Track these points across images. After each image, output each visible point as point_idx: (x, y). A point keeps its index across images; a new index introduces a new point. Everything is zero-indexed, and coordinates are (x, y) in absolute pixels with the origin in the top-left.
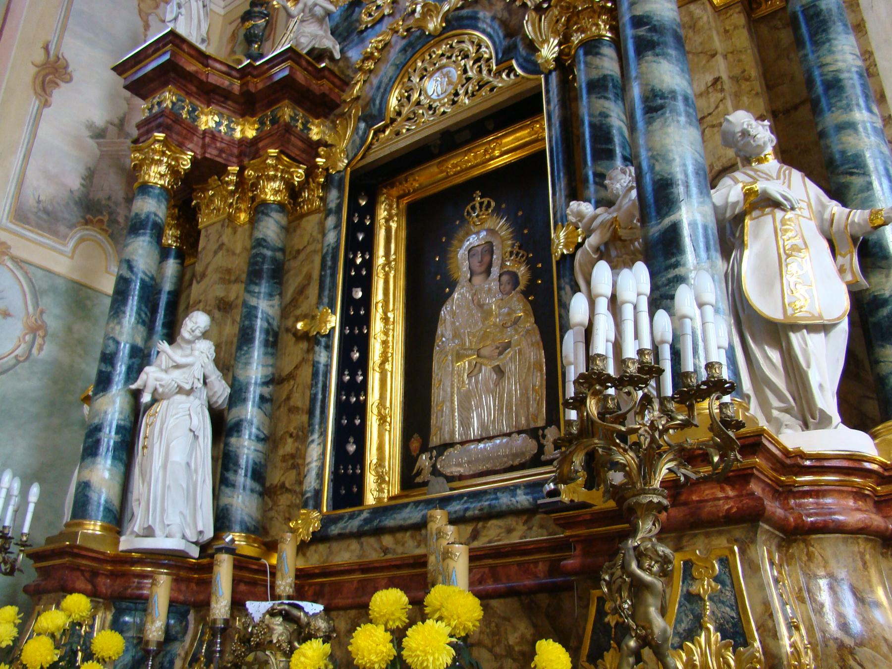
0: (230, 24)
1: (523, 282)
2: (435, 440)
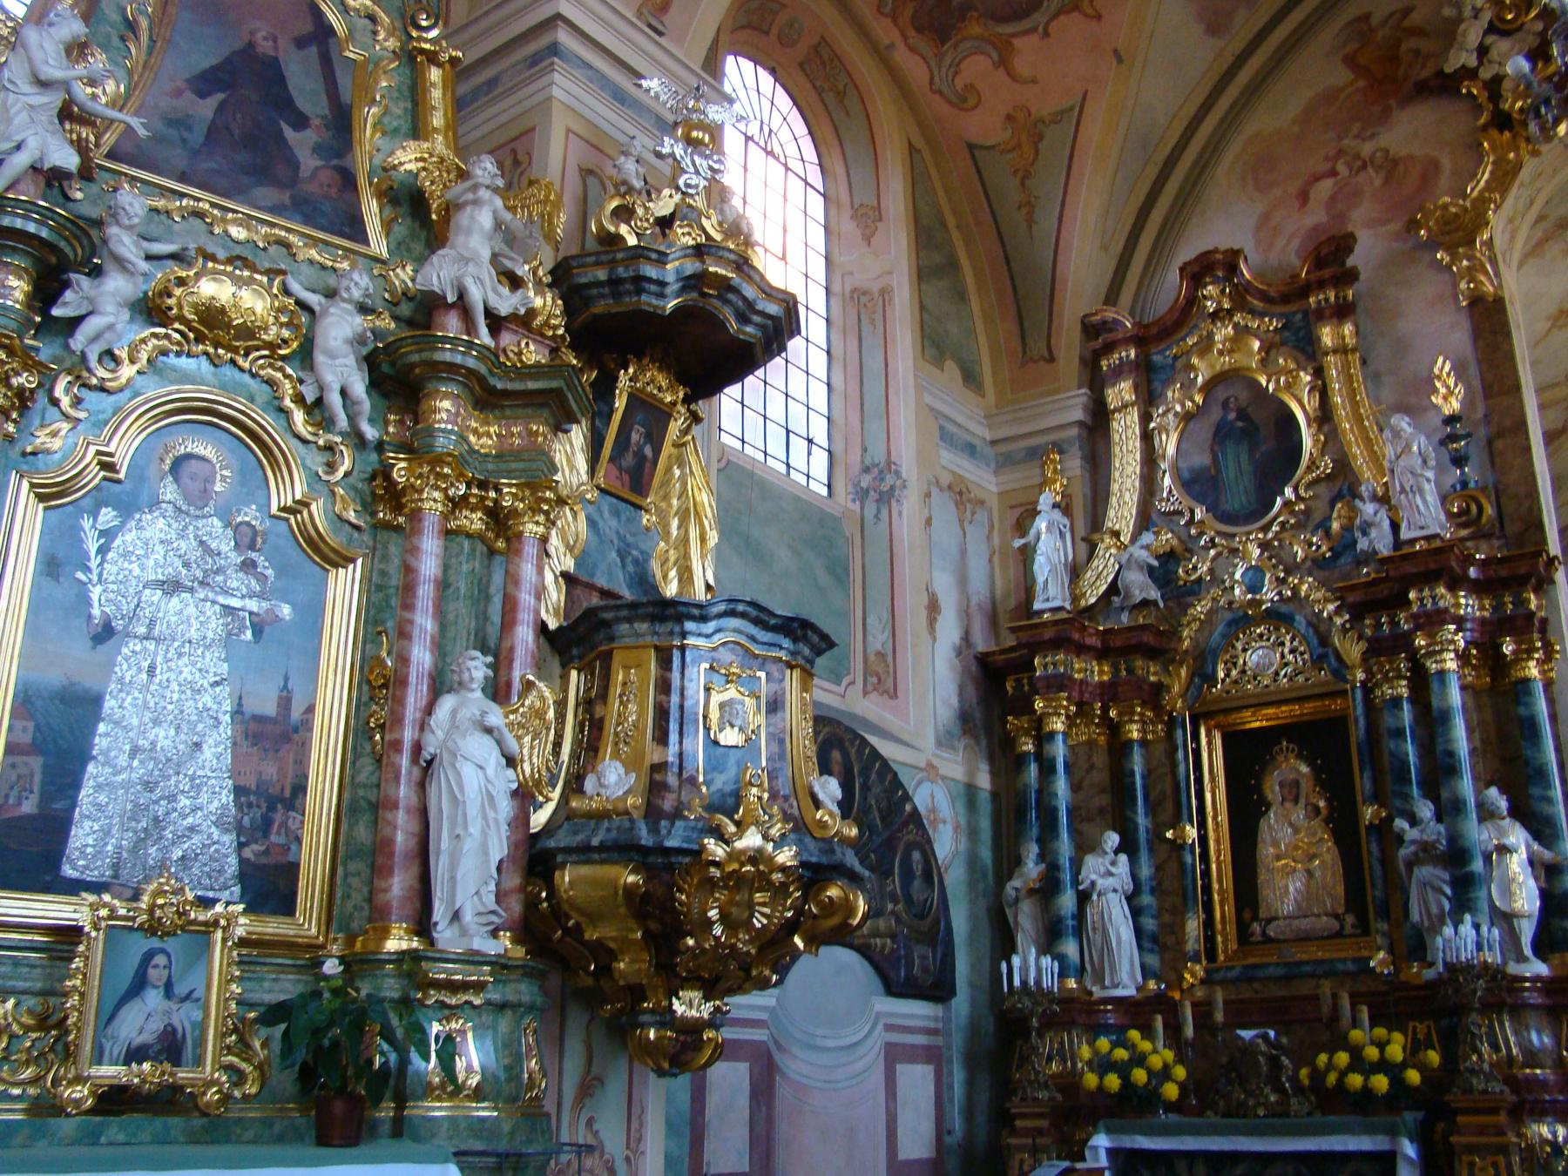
0: (1012, 507)
1: (1324, 812)
2: (1262, 914)
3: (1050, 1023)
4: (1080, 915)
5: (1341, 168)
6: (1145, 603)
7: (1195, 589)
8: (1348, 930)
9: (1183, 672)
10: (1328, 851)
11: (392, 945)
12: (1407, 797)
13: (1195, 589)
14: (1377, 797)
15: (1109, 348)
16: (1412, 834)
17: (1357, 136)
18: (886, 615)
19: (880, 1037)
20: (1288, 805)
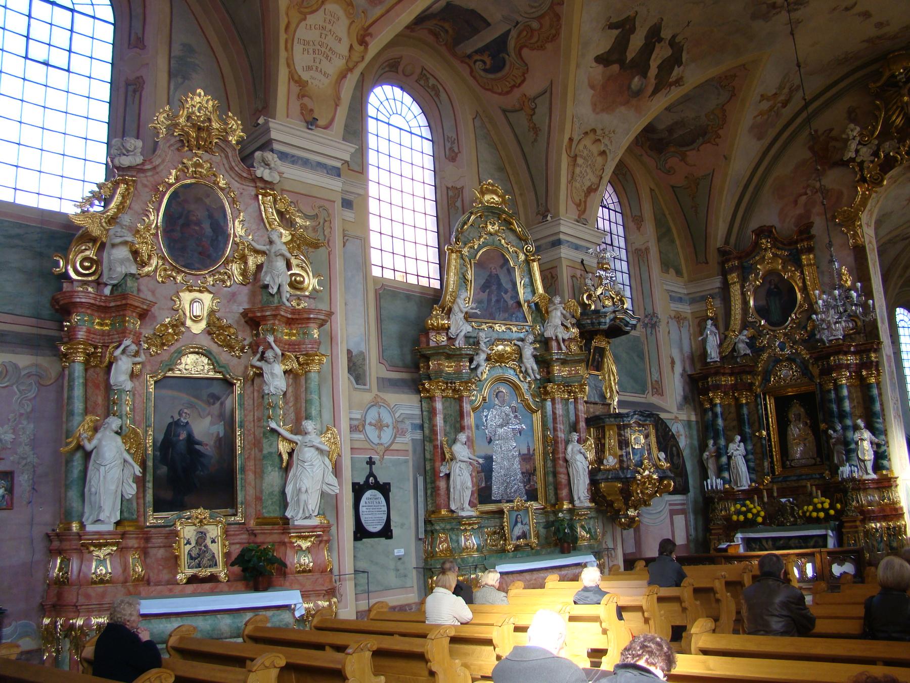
0: (696, 318)
2: (790, 458)
3: (721, 499)
4: (729, 464)
5: (808, 192)
6: (745, 355)
7: (763, 349)
8: (818, 463)
9: (759, 378)
10: (811, 438)
11: (565, 507)
12: (833, 422)
13: (763, 349)
14: (824, 421)
15: (728, 261)
16: (834, 435)
17: (814, 180)
18: (657, 368)
19: (668, 508)
20: (797, 422)
